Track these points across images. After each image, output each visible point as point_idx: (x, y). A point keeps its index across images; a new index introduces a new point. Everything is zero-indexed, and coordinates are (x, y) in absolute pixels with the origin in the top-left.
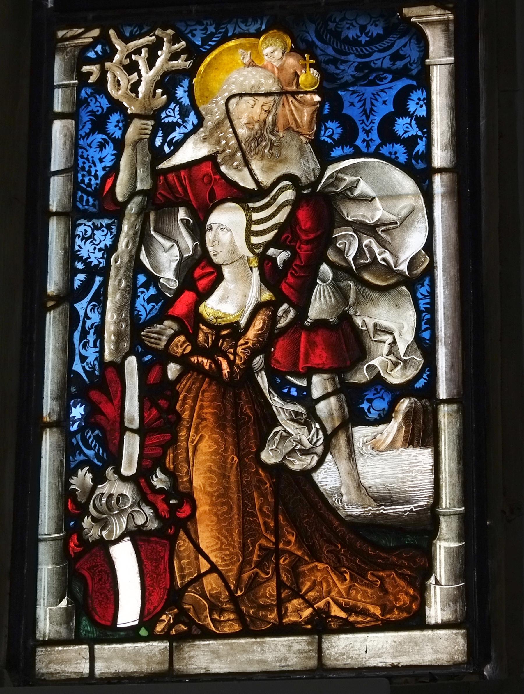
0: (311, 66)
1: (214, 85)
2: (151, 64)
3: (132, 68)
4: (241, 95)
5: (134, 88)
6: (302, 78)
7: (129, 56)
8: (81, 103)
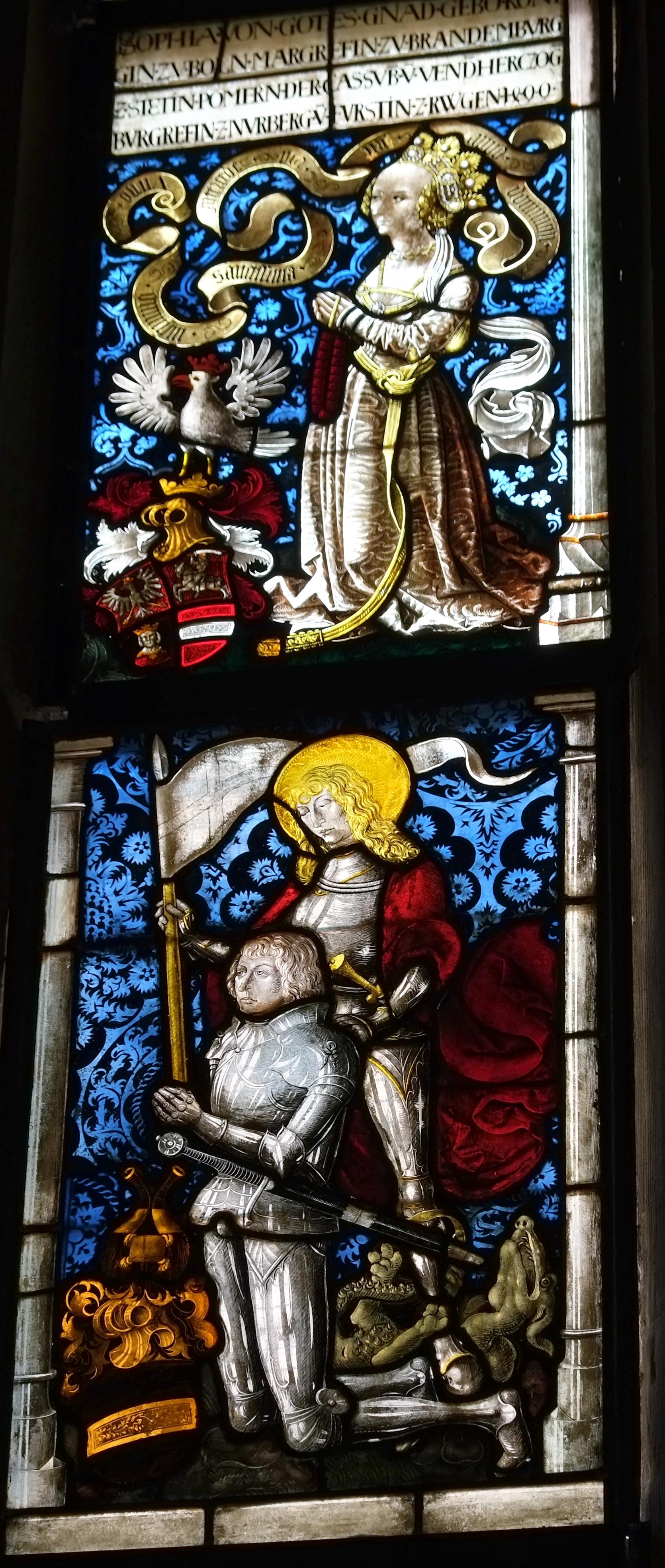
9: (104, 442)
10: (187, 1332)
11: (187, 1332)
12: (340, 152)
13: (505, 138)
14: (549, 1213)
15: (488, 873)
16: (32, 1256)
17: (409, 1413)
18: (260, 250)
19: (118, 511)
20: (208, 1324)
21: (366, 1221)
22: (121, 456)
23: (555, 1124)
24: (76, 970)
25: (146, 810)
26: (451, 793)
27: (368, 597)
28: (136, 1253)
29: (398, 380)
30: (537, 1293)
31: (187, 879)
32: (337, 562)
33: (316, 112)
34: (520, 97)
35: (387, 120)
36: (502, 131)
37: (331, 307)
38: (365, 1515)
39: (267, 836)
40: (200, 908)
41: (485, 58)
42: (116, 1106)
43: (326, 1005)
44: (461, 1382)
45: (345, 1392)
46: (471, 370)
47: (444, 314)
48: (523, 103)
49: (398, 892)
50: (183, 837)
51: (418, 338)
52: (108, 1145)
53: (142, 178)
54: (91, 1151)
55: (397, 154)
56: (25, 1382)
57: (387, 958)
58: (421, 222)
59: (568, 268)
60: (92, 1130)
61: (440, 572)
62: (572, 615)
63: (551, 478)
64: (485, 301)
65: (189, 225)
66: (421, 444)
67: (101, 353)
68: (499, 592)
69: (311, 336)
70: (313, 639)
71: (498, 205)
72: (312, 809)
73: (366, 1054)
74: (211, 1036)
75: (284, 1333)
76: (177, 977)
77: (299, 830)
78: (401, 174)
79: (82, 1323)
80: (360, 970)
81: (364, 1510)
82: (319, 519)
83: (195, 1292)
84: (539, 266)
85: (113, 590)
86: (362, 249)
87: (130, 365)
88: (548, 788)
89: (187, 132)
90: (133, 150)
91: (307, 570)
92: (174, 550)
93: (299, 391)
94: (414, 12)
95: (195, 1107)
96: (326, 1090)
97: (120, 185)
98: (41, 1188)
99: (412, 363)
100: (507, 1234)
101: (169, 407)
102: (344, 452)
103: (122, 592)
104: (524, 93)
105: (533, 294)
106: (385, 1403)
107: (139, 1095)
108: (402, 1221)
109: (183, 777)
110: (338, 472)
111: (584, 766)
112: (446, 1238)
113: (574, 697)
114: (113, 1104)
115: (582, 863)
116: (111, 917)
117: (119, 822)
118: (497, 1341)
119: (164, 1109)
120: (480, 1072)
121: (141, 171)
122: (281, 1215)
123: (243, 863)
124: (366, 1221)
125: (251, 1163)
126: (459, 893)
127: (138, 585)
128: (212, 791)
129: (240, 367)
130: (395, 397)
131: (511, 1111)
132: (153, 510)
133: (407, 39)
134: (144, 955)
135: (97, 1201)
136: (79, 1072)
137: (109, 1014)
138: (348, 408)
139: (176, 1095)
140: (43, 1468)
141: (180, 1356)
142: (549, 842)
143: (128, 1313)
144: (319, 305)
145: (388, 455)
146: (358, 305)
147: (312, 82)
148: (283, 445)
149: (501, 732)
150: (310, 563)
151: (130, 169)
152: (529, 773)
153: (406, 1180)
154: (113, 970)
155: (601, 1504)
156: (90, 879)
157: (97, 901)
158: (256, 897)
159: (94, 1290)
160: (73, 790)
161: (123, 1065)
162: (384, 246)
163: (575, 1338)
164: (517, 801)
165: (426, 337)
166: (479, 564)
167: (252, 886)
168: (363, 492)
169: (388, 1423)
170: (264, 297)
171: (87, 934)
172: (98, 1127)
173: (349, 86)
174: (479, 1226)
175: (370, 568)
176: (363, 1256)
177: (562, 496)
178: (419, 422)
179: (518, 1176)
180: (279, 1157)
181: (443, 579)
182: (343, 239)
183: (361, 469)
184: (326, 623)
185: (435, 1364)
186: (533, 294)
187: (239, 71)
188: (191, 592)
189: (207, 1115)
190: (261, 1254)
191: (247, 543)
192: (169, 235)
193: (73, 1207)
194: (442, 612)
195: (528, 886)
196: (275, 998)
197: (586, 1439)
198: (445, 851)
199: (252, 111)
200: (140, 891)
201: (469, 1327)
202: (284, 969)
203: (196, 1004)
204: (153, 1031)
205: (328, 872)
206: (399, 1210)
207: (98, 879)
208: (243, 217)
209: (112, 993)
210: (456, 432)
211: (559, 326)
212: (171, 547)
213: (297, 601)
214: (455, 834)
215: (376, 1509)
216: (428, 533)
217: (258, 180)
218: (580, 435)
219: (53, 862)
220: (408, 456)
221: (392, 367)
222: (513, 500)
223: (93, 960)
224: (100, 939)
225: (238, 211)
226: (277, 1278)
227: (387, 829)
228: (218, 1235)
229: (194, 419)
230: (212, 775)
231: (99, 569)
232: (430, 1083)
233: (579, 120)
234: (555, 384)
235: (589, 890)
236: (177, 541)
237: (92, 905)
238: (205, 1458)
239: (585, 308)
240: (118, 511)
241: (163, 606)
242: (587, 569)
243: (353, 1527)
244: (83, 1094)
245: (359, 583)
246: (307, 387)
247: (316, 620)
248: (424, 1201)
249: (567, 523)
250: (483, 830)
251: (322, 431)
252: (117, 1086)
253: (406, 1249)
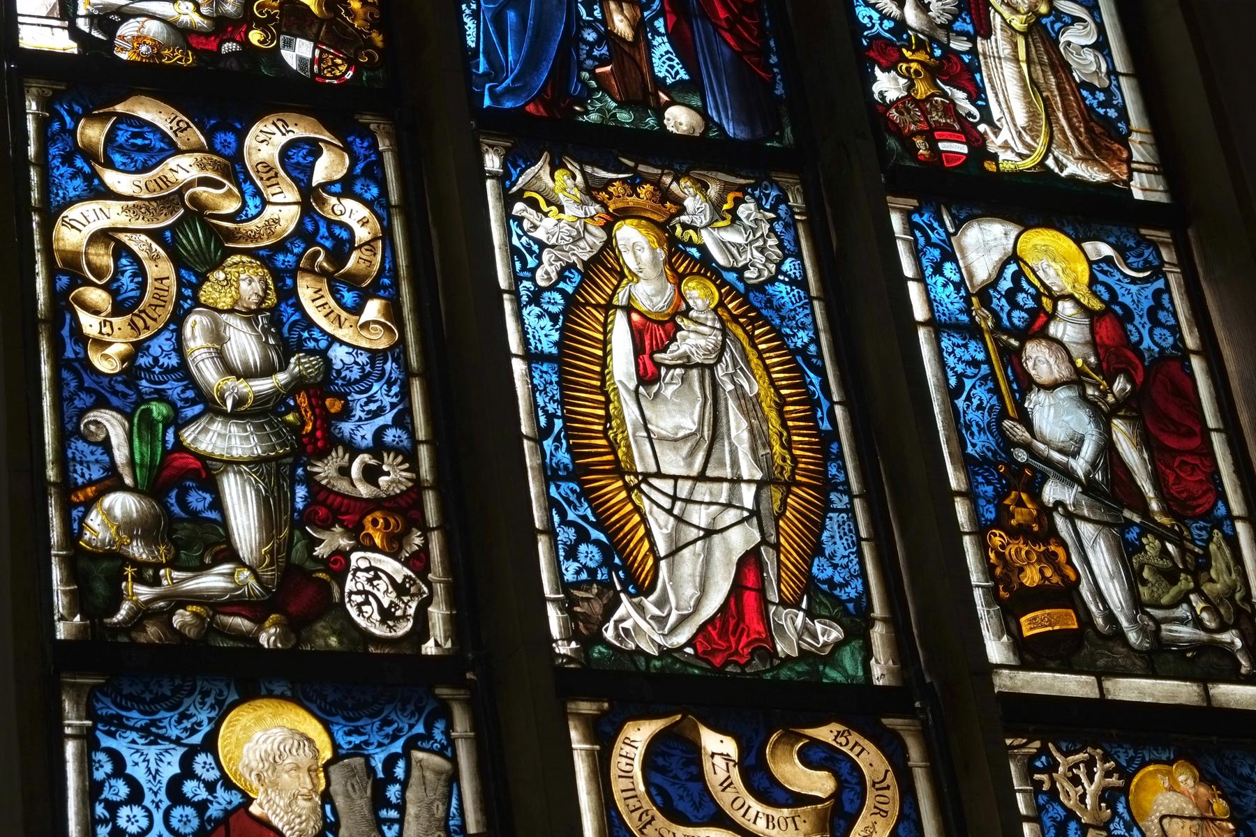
0: (1220, 796)
1: (1146, 805)
2: (1091, 781)
3: (1075, 781)
4: (1172, 816)
5: (1082, 798)
6: (1215, 806)
7: (1070, 769)
8: (1040, 809)
10: (1058, 569)
16: (961, 509)
21: (1137, 520)
24: (938, 340)
29: (1018, 22)
31: (984, 294)
40: (996, 315)
45: (1151, 617)
79: (1000, 556)
80: (1092, 369)
82: (997, 95)
88: (1160, 284)
95: (1027, 434)
100: (1210, 539)
106: (1174, 628)
108: (1155, 522)
113: (1160, 234)
115: (1191, 332)
118: (1221, 600)
120: (1172, 442)
122: (1090, 508)
125: (1067, 475)
130: (1021, 33)
131: (1194, 468)
134: (973, 337)
135: (989, 483)
143: (1023, 553)
145: (1024, 66)
169: (1179, 640)
175: (1032, 129)
177: (1123, 111)
179: (1207, 506)
184: (1017, 159)
202: (1052, 361)
204: (990, 385)
215: (1185, 690)
216: (1057, 118)
232: (1145, 441)
234: (1101, 46)
236: (922, 89)
246: (969, 13)
253: (1162, 539)
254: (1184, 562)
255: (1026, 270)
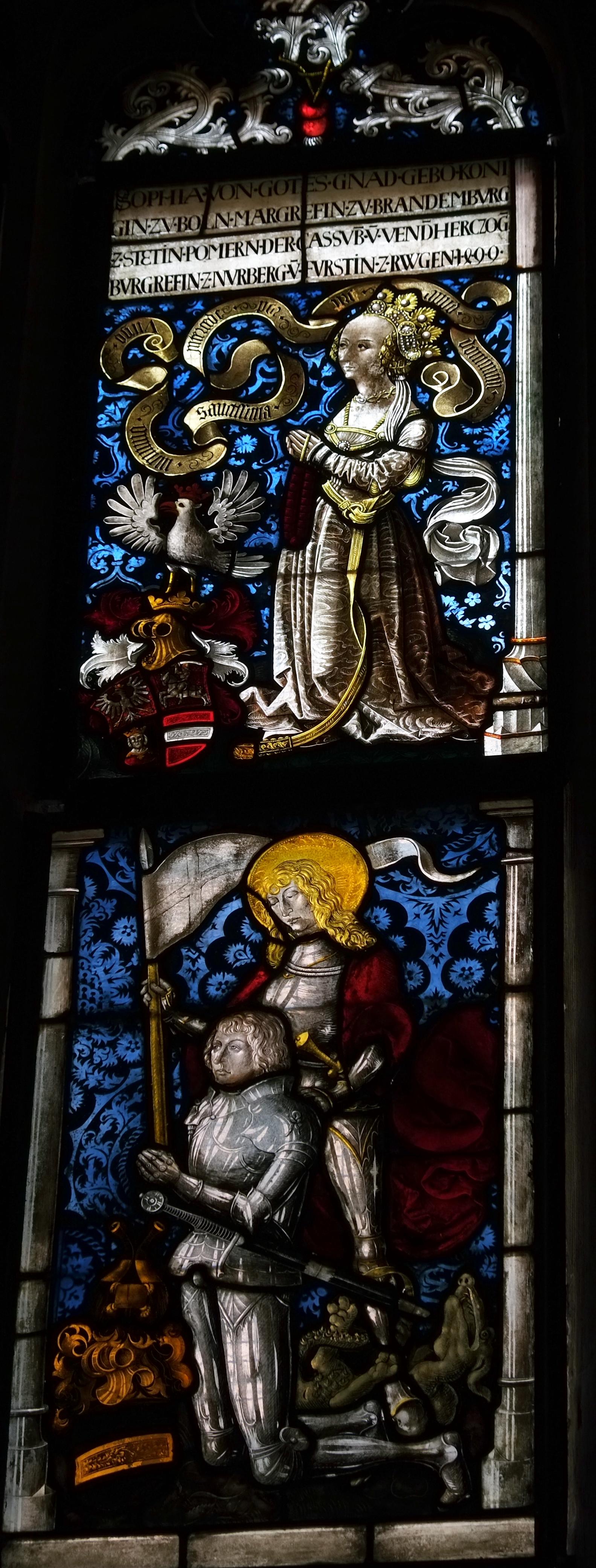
9: (99, 560)
10: (165, 1373)
11: (165, 1373)
12: (312, 303)
13: (457, 295)
14: (487, 1271)
15: (437, 961)
16: (27, 1300)
17: (362, 1451)
18: (240, 390)
19: (110, 623)
20: (184, 1366)
21: (326, 1276)
22: (114, 573)
23: (494, 1191)
25: (133, 896)
26: (405, 888)
27: (332, 707)
28: (121, 1300)
29: (360, 513)
30: (476, 1345)
32: (305, 675)
33: (290, 266)
34: (472, 259)
35: (353, 276)
36: (456, 288)
37: (302, 442)
38: (322, 1544)
39: (240, 923)
40: (180, 987)
41: (441, 223)
42: (104, 1165)
43: (292, 1079)
44: (408, 1424)
45: (305, 1430)
46: (426, 504)
47: (403, 453)
48: (474, 264)
49: (357, 977)
50: (165, 922)
51: (378, 473)
52: (97, 1201)
53: (135, 322)
54: (81, 1206)
55: (362, 307)
56: (21, 1415)
57: (346, 1037)
58: (382, 368)
59: (513, 415)
60: (83, 1186)
61: (397, 687)
62: (514, 729)
63: (497, 604)
64: (439, 442)
65: (176, 365)
66: (381, 570)
67: (97, 479)
68: (449, 707)
69: (283, 470)
70: (282, 745)
71: (451, 355)
72: (281, 899)
73: (327, 1124)
74: (190, 1104)
75: (252, 1374)
76: (159, 1049)
77: (269, 918)
78: (365, 323)
79: (71, 1363)
81: (322, 1539)
82: (289, 636)
83: (172, 1337)
84: (488, 411)
85: (105, 695)
86: (330, 391)
87: (123, 492)
88: (491, 886)
89: (176, 282)
90: (128, 296)
91: (278, 681)
92: (160, 660)
93: (273, 519)
94: (378, 179)
95: (175, 1168)
96: (291, 1155)
97: (116, 327)
98: (37, 1238)
99: (374, 496)
100: (450, 1290)
101: (156, 530)
102: (312, 575)
103: (113, 698)
104: (475, 255)
105: (481, 436)
106: (341, 1442)
107: (125, 1155)
109: (167, 868)
110: (307, 593)
111: (523, 867)
112: (396, 1292)
113: (514, 804)
114: (102, 1163)
116: (101, 992)
117: (109, 906)
118: (441, 1387)
119: (147, 1170)
121: (135, 316)
122: (249, 1269)
123: (220, 946)
124: (326, 1276)
125: (224, 1220)
126: (411, 979)
127: (128, 691)
128: (192, 880)
129: (220, 496)
130: (358, 527)
132: (142, 623)
133: (372, 204)
134: (130, 1029)
135: (86, 1251)
136: (72, 1133)
137: (99, 1081)
138: (317, 536)
139: (158, 1157)
140: (36, 1495)
141: (159, 1394)
142: (491, 935)
143: (113, 1355)
144: (291, 442)
145: (352, 579)
146: (326, 442)
147: (287, 239)
148: (258, 569)
149: (450, 833)
150: (282, 675)
151: (125, 313)
152: (474, 872)
153: (362, 1239)
154: (102, 1042)
155: (532, 1538)
156: (83, 958)
157: (88, 978)
158: (230, 978)
159: (83, 1333)
160: (68, 877)
161: (110, 1128)
162: (348, 391)
163: (511, 1386)
164: (463, 897)
165: (386, 473)
166: (431, 680)
167: (227, 968)
168: (329, 613)
169: (345, 1460)
170: (243, 433)
171: (80, 1008)
172: (88, 1185)
173: (321, 245)
174: (426, 1282)
175: (334, 679)
176: (323, 1307)
177: (506, 619)
178: (379, 550)
180: (248, 1214)
181: (400, 694)
182: (313, 382)
183: (327, 591)
185: (386, 1407)
186: (481, 436)
187: (222, 228)
188: (175, 699)
189: (185, 1176)
190: (232, 1304)
191: (226, 656)
192: (159, 374)
193: (64, 1257)
194: (398, 723)
195: (472, 974)
196: (247, 1070)
197: (519, 1479)
198: (399, 941)
199: (233, 264)
200: (127, 970)
201: (416, 1374)
202: (255, 1044)
203: (176, 1074)
204: (137, 1097)
205: (295, 957)
206: (355, 1266)
207: (89, 958)
208: (224, 359)
209: (101, 1062)
210: (412, 559)
211: (504, 467)
212: (158, 657)
213: (269, 710)
214: (408, 925)
215: (332, 1538)
216: (387, 651)
217: (238, 326)
218: (522, 566)
219: (50, 942)
220: (369, 581)
221: (355, 499)
222: (461, 622)
223: (85, 1032)
224: (91, 1013)
225: (220, 354)
226: (246, 1326)
227: (347, 919)
228: (194, 1285)
229: (177, 541)
230: (193, 866)
231: (93, 675)
233: (523, 281)
234: (501, 519)
235: (526, 979)
236: (162, 652)
237: (84, 981)
238: (181, 1488)
239: (527, 451)
240: (110, 623)
241: (149, 711)
242: (527, 688)
243: (312, 1554)
244: (74, 1153)
245: (324, 695)
247: (285, 728)
248: (377, 1258)
249: (510, 644)
250: (432, 922)
251: (293, 556)
252: (105, 1147)
254: (391, 1332)
255: (256, 906)
